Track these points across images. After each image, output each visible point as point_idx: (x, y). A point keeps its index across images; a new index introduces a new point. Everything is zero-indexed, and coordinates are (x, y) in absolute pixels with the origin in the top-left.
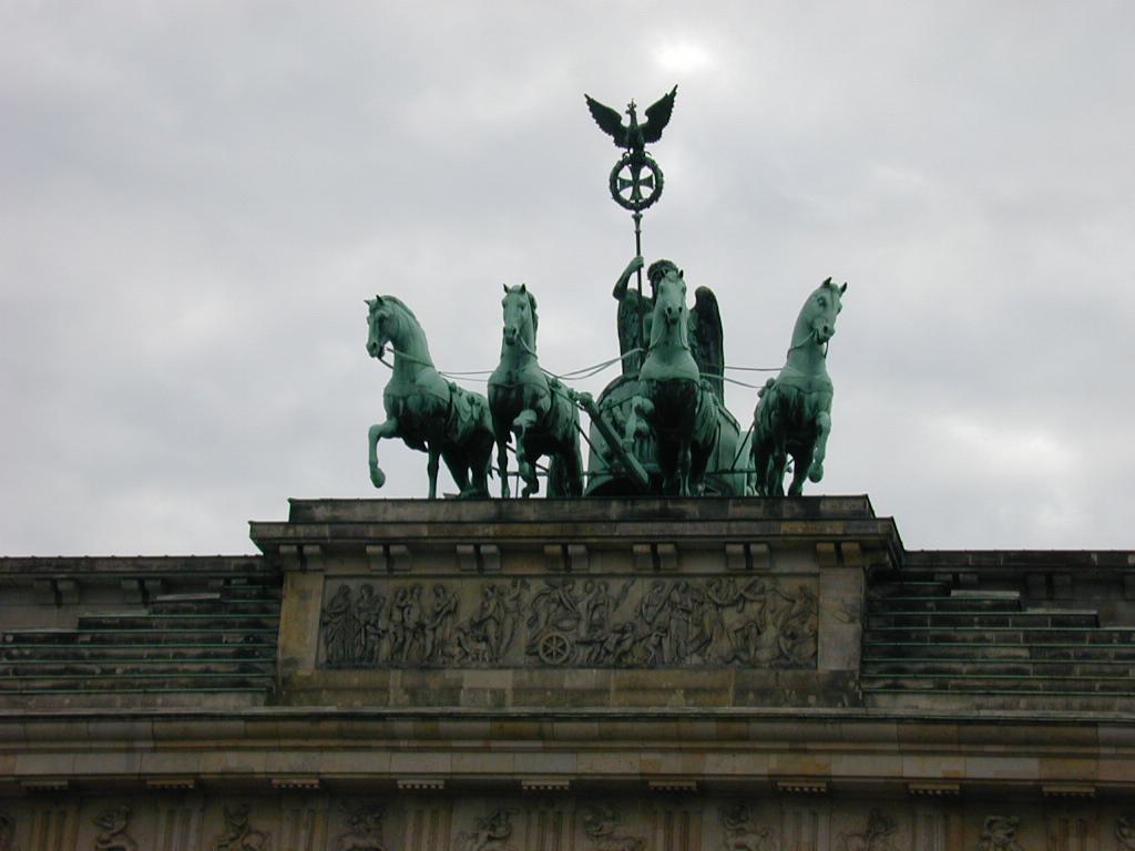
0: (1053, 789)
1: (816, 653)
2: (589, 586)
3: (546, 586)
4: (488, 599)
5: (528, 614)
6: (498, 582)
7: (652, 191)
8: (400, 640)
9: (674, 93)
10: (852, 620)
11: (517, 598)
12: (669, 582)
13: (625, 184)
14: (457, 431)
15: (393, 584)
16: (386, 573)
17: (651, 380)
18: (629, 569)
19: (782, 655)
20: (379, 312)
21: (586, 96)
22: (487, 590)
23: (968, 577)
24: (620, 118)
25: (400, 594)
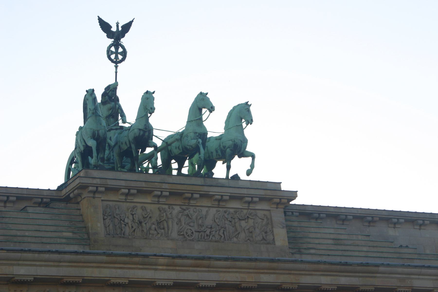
0: (363, 288)
1: (274, 239)
2: (195, 210)
3: (180, 209)
5: (176, 220)
6: (164, 206)
7: (122, 57)
9: (132, 21)
11: (171, 213)
12: (221, 209)
13: (112, 53)
15: (124, 206)
16: (124, 200)
17: (196, 133)
18: (210, 205)
19: (263, 239)
20: (93, 96)
21: (98, 17)
24: (111, 27)
25: (130, 209)
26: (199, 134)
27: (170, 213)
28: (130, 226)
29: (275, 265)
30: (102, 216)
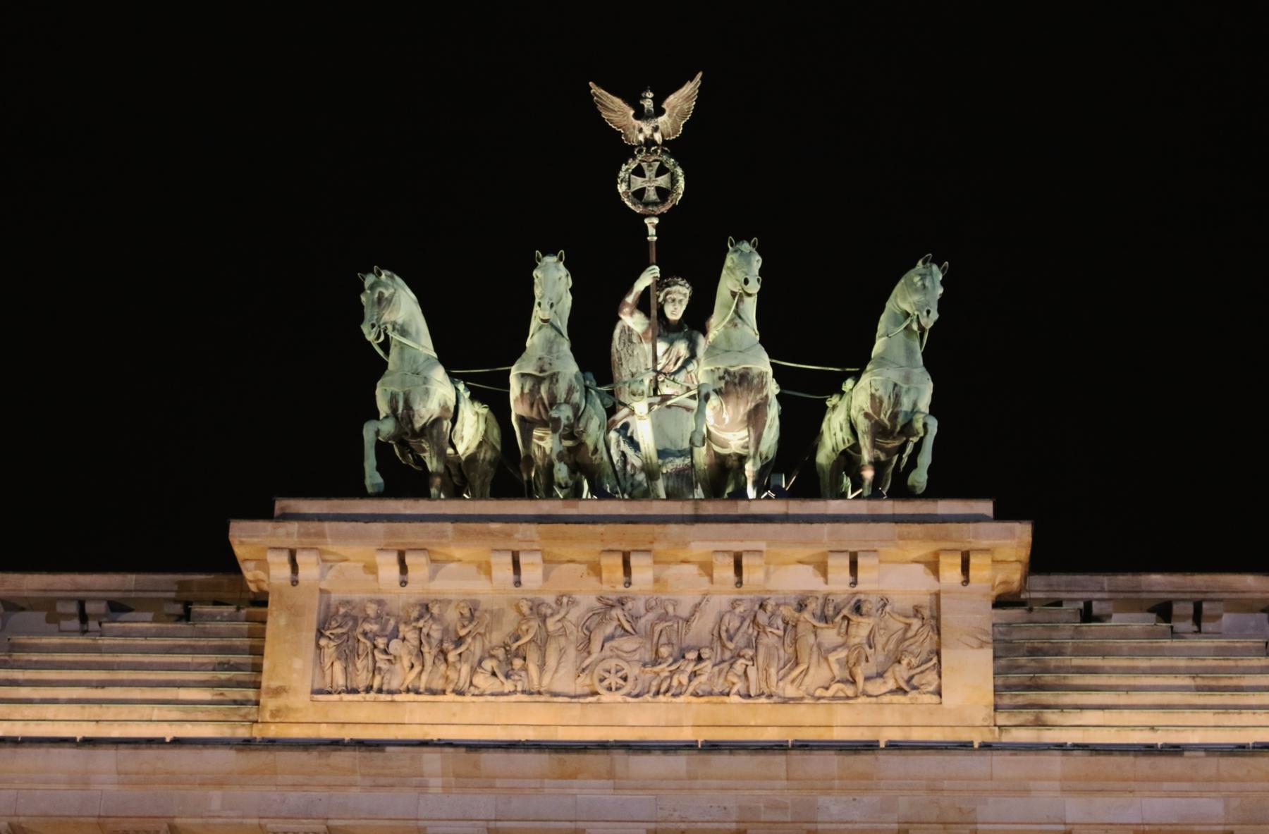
4: (529, 620)
8: (417, 669)
10: (981, 647)
14: (462, 438)
22: (525, 610)
23: (1104, 605)
25: (415, 614)
26: (726, 372)
27: (558, 617)
28: (406, 664)
29: (862, 762)
30: (313, 634)
